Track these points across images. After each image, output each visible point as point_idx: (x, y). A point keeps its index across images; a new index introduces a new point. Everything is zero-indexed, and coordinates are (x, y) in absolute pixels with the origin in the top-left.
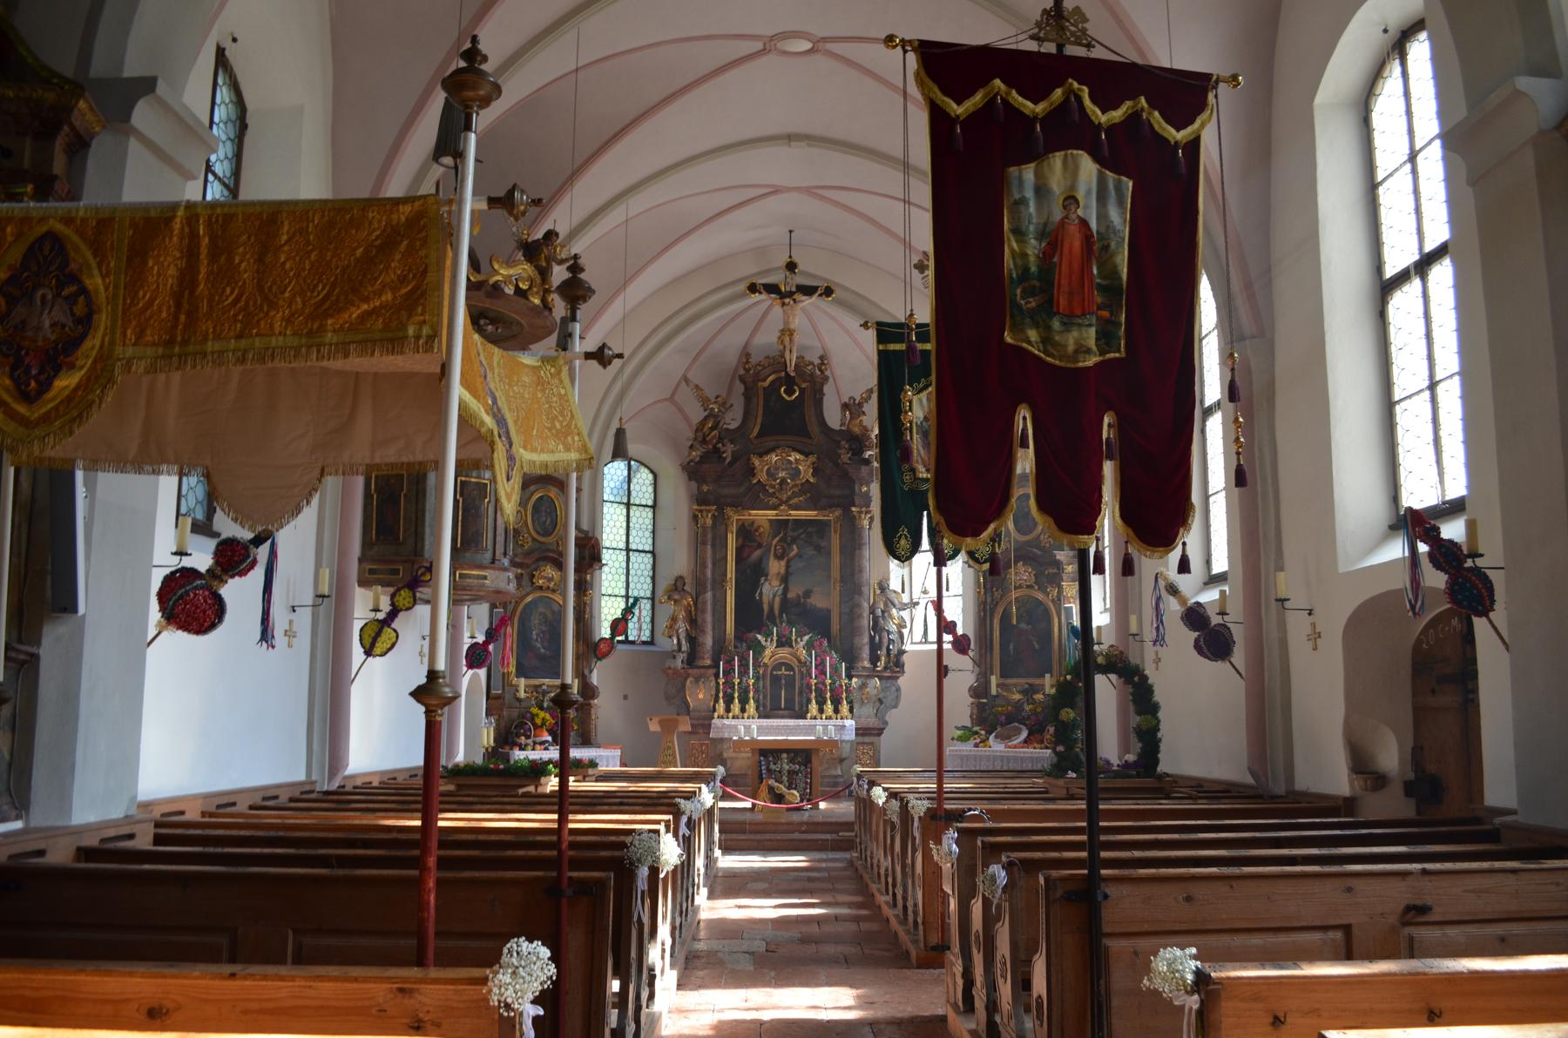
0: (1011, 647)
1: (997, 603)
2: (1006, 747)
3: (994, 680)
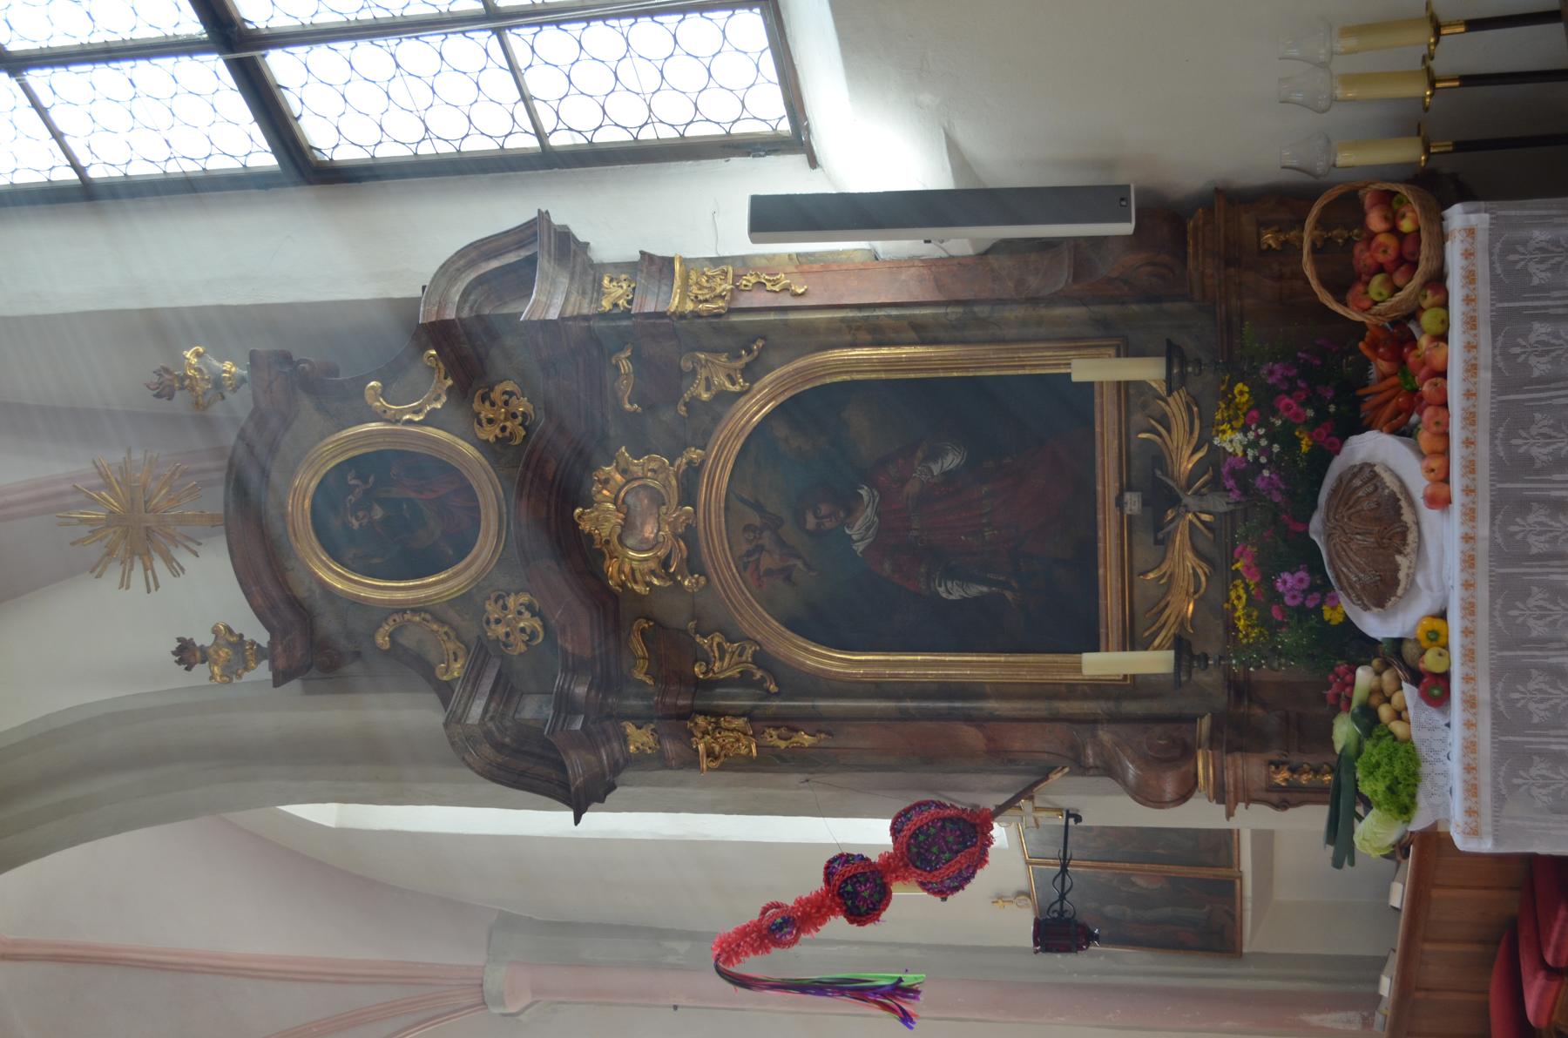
0: (952, 591)
1: (762, 659)
2: (1440, 501)
3: (1099, 664)
